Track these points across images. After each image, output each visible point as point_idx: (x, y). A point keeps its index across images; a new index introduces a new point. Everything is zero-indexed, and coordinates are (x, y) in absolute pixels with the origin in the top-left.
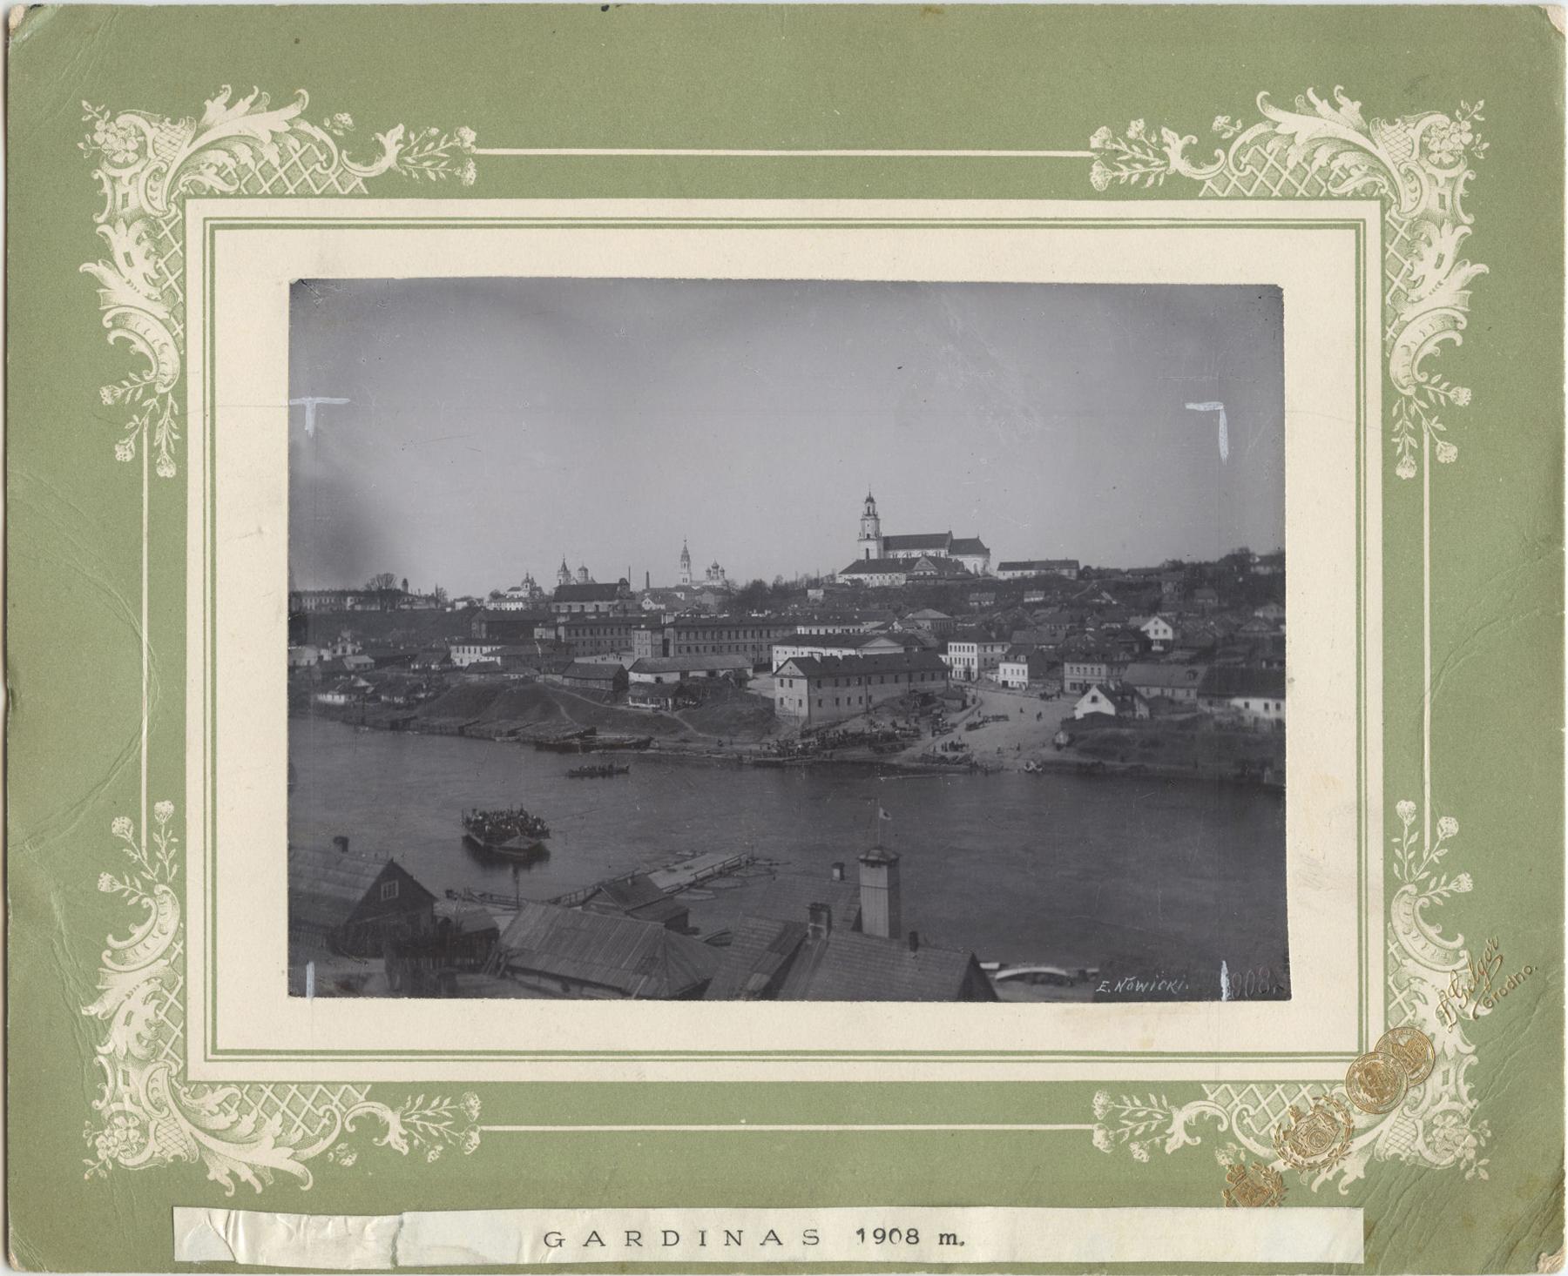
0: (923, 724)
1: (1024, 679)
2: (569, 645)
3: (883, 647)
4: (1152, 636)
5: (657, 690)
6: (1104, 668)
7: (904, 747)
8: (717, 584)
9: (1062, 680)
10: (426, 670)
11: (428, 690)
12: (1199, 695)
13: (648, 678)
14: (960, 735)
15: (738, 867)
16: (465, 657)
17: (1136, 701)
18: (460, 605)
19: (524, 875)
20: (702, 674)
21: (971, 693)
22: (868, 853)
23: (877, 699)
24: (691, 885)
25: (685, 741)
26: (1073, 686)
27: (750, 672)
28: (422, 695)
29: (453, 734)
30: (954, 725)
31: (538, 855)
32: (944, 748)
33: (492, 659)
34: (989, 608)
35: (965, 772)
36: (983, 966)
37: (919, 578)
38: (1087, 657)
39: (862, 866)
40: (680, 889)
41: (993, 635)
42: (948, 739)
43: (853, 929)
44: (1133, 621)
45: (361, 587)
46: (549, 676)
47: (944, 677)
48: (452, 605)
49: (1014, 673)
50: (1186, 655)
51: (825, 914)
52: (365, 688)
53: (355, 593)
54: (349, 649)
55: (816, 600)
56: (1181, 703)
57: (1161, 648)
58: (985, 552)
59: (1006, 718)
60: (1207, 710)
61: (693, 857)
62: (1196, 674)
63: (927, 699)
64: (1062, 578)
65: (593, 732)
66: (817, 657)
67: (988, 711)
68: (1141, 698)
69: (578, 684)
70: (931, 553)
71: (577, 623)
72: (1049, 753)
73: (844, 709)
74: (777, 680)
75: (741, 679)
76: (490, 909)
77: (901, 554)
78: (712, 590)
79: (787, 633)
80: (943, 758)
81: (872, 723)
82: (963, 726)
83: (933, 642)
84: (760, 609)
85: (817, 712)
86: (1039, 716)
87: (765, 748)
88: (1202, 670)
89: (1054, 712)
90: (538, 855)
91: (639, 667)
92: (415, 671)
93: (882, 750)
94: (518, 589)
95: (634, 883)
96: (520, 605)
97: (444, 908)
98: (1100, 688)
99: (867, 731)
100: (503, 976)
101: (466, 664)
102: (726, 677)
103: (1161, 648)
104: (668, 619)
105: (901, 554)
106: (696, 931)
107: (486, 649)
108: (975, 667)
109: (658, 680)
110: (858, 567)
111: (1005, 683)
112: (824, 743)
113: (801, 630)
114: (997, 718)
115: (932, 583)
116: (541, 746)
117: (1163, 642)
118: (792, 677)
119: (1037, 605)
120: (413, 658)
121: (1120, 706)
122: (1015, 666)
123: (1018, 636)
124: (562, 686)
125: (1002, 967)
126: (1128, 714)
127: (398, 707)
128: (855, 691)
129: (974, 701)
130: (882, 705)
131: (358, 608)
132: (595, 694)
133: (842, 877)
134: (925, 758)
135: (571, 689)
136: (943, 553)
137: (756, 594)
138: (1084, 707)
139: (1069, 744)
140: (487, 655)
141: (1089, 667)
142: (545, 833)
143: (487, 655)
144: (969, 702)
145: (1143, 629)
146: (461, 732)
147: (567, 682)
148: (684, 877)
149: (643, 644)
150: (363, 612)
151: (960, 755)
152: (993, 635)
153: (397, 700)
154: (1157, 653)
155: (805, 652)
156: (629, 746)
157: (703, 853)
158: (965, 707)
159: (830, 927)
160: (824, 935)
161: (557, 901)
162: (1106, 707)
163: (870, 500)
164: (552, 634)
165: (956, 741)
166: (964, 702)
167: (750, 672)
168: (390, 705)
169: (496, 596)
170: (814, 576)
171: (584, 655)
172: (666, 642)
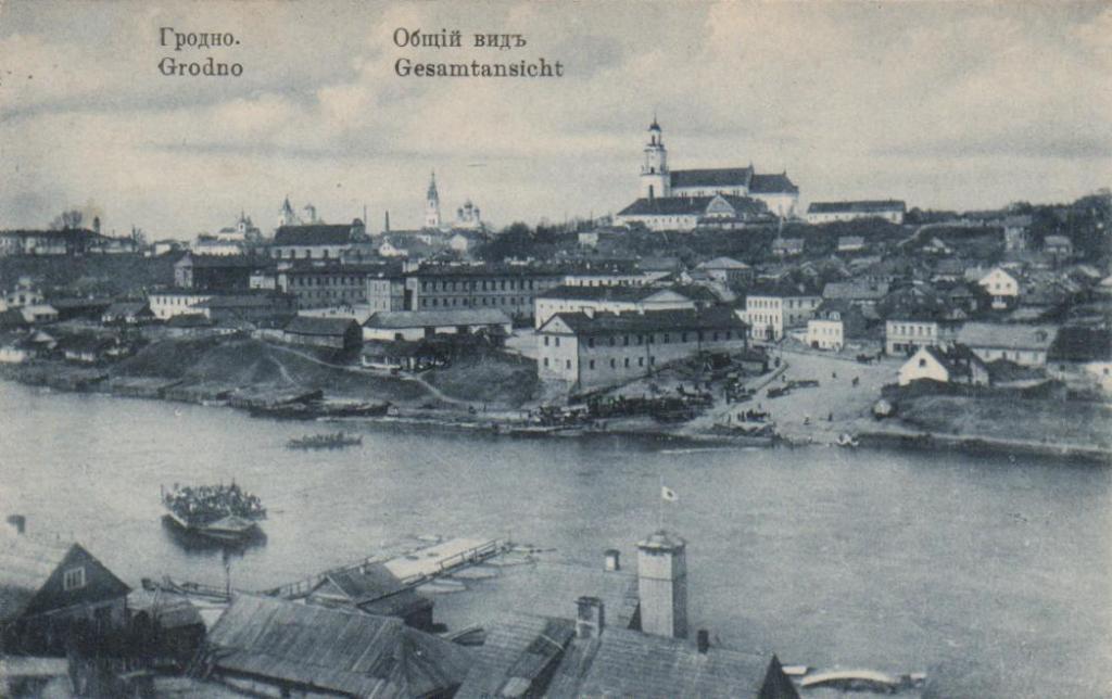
0: (715, 391)
1: (840, 339)
2: (290, 299)
3: (667, 301)
4: (992, 291)
5: (397, 350)
6: (934, 326)
7: (692, 416)
8: (472, 225)
9: (883, 340)
10: (120, 322)
11: (122, 345)
12: (1049, 359)
13: (388, 335)
14: (759, 402)
15: (492, 554)
16: (166, 307)
17: (973, 366)
18: (162, 249)
19: (236, 563)
20: (453, 330)
21: (774, 354)
22: (649, 539)
23: (661, 360)
24: (435, 575)
25: (429, 406)
26: (897, 347)
27: (508, 329)
28: (115, 352)
29: (152, 397)
30: (753, 391)
31: (252, 538)
32: (741, 417)
33: (199, 311)
34: (797, 257)
35: (766, 446)
36: (787, 670)
37: (713, 220)
38: (919, 313)
39: (642, 555)
40: (423, 580)
41: (802, 288)
42: (744, 408)
43: (630, 627)
44: (970, 274)
45: (43, 226)
46: (268, 332)
47: (741, 336)
48: (152, 248)
49: (828, 332)
50: (1033, 313)
51: (595, 610)
52: (45, 343)
53: (36, 234)
54: (29, 297)
55: (589, 246)
56: (1026, 368)
57: (1003, 305)
58: (793, 190)
59: (815, 383)
60: (1060, 375)
61: (439, 542)
62: (1044, 336)
63: (721, 361)
64: (884, 222)
65: (319, 395)
66: (589, 314)
67: (790, 377)
68: (979, 362)
69: (302, 340)
70: (728, 190)
71: (302, 270)
72: (874, 428)
73: (621, 372)
74: (541, 338)
75: (496, 336)
76: (196, 602)
77: (692, 192)
78: (465, 233)
79: (553, 285)
80: (739, 430)
81: (654, 389)
82: (764, 392)
83: (728, 296)
84: (521, 255)
85: (587, 372)
86: (855, 382)
87: (525, 416)
88: (1052, 332)
89: (874, 378)
90: (252, 538)
91: (373, 322)
92: (107, 324)
93: (667, 420)
94: (231, 231)
95: (368, 573)
96: (234, 250)
97: (139, 600)
98: (930, 349)
99: (649, 396)
100: (210, 679)
101: (167, 316)
102: (481, 332)
103: (1003, 305)
104: (412, 267)
105: (692, 192)
106: (442, 628)
107: (193, 300)
108: (778, 327)
109: (398, 336)
110: (643, 206)
111: (815, 345)
112: (596, 411)
113: (570, 281)
114: (804, 384)
115: (727, 226)
116: (257, 411)
117: (1007, 298)
118: (558, 335)
119: (854, 254)
120: (102, 310)
121: (954, 371)
122: (828, 325)
123: (832, 290)
124: (282, 343)
125: (810, 671)
126: (964, 380)
127: (87, 365)
128: (634, 353)
129: (777, 363)
130: (666, 367)
131: (40, 250)
132: (324, 353)
133: (617, 567)
134: (718, 429)
135: (292, 346)
136: (742, 191)
137: (517, 239)
138: (910, 372)
139: (891, 415)
140: (195, 306)
141: (916, 326)
142: (261, 513)
143: (195, 306)
144: (771, 365)
145: (982, 283)
146: (160, 395)
147: (288, 338)
148: (427, 566)
149: (380, 295)
150: (46, 256)
151: (760, 426)
152: (802, 288)
153: (84, 357)
154: (1000, 311)
155: (573, 306)
156: (361, 413)
157: (450, 538)
158: (766, 370)
159: (602, 625)
160: (595, 634)
161: (275, 593)
162: (938, 372)
163: (655, 127)
164: (270, 284)
165: (756, 410)
166: (766, 365)
167: (508, 329)
168: (73, 362)
169: (205, 239)
170: (586, 218)
171: (310, 308)
172: (408, 294)
